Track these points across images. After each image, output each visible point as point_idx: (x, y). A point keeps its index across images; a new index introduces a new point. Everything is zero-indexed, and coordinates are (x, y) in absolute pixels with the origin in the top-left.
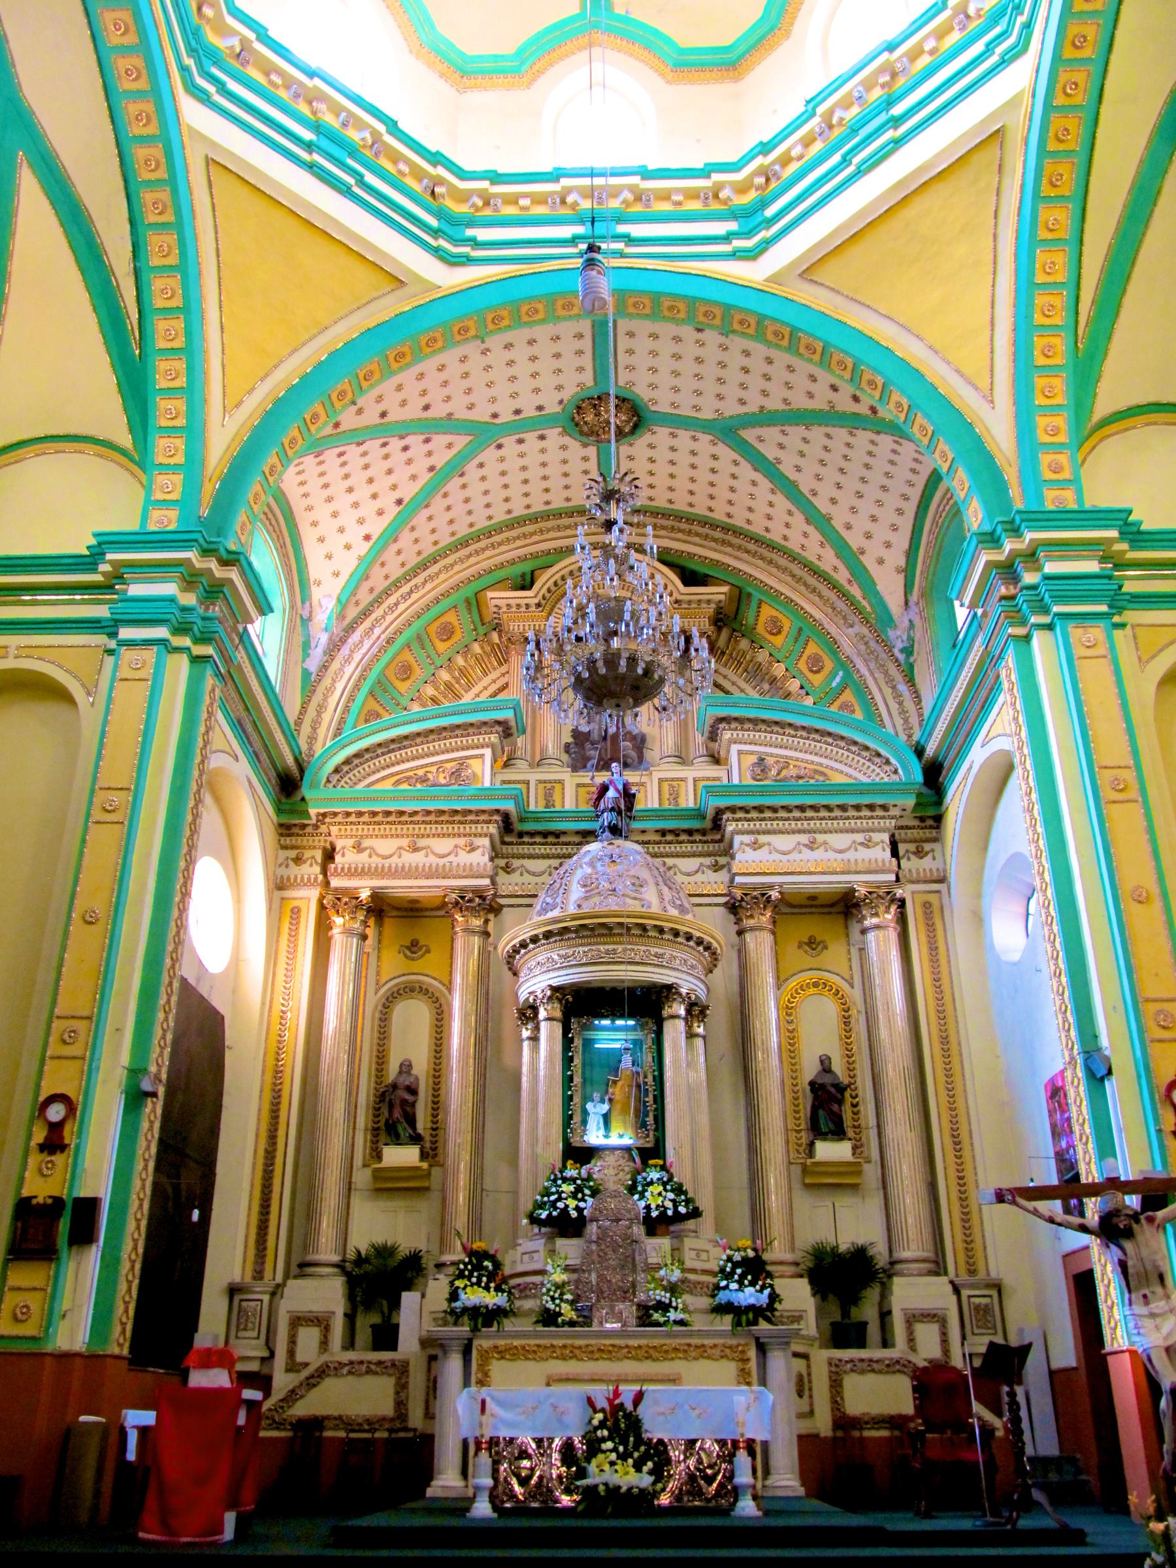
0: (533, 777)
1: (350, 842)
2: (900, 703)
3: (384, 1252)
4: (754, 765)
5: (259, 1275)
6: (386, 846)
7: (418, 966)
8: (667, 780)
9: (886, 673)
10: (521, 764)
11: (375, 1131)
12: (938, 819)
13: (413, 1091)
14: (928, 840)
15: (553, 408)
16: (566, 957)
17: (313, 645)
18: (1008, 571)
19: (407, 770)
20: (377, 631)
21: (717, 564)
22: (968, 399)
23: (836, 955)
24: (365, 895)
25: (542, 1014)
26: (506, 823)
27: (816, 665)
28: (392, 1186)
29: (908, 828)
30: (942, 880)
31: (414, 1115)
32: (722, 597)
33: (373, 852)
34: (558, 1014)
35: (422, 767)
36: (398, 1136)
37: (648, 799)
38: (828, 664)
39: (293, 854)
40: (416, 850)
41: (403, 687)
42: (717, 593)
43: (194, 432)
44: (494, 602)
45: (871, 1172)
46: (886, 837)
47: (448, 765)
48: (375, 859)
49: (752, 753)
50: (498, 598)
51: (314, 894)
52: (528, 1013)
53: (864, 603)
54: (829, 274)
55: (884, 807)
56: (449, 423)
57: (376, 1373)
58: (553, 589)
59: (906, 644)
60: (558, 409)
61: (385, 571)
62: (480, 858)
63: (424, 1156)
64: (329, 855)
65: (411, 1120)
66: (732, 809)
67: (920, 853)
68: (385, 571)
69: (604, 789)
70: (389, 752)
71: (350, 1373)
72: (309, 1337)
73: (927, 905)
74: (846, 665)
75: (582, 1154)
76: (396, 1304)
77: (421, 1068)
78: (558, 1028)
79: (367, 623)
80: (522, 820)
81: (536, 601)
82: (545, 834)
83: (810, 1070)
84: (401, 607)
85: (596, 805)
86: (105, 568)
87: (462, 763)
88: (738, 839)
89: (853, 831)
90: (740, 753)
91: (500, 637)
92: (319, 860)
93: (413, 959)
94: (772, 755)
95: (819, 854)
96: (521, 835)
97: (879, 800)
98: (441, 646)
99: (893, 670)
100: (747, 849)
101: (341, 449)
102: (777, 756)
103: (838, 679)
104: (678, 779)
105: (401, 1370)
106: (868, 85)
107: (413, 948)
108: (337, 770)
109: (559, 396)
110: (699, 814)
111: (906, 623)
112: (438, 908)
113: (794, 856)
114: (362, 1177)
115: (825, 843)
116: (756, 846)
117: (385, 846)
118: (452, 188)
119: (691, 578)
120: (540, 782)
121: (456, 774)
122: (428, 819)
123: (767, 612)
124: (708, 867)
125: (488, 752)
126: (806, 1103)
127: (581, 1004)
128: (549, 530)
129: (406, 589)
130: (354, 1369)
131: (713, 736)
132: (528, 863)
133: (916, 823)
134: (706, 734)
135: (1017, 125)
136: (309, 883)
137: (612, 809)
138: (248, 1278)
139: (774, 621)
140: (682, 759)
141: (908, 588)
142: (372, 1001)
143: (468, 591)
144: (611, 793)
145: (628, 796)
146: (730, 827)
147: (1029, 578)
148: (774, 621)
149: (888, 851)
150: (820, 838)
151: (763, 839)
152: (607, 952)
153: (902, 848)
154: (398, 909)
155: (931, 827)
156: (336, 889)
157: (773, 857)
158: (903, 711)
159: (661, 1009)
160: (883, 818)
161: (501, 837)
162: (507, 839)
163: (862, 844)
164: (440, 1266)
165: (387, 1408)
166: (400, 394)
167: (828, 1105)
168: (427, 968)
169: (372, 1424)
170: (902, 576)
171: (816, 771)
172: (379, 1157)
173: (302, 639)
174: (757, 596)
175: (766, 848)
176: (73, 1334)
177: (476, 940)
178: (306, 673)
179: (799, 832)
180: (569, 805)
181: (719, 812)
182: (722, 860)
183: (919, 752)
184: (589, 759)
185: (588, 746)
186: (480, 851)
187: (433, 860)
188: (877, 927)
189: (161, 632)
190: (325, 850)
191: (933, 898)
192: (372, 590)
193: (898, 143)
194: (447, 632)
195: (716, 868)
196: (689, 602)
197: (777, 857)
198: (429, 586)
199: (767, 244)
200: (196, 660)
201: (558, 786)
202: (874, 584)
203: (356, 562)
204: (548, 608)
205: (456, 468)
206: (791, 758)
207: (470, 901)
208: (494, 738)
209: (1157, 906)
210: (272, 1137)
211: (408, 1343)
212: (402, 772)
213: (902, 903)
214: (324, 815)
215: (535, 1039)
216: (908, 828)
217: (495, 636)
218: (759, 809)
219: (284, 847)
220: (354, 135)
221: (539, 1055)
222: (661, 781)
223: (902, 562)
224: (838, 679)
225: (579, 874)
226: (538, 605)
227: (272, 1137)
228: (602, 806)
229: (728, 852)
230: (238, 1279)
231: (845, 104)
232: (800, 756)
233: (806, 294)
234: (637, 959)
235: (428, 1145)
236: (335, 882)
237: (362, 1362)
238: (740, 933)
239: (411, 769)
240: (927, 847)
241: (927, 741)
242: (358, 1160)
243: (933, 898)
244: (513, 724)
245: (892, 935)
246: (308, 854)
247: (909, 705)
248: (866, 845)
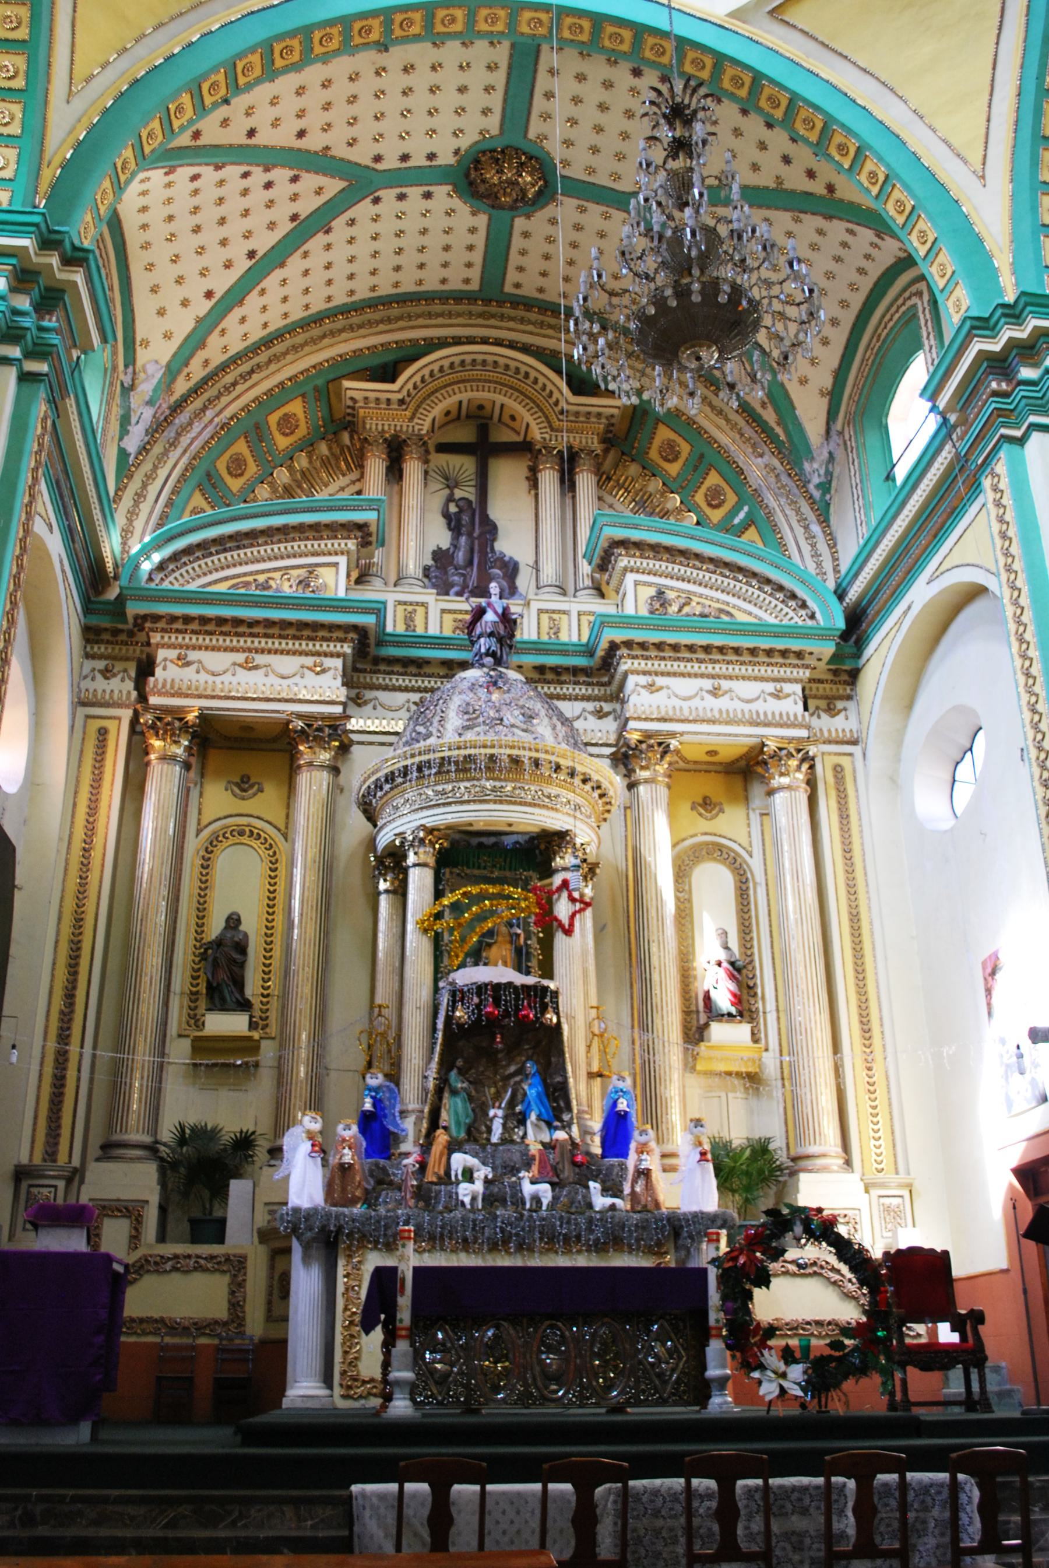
0: (391, 598)
2: (813, 546)
4: (652, 598)
5: (51, 1154)
8: (547, 611)
9: (798, 511)
10: (377, 583)
11: (194, 996)
12: (854, 675)
13: (242, 948)
14: (841, 698)
15: (447, 158)
16: (444, 793)
17: (133, 420)
19: (245, 574)
20: (210, 414)
24: (191, 717)
25: (411, 859)
29: (820, 681)
31: (243, 977)
32: (615, 411)
33: (201, 667)
35: (263, 572)
36: (223, 999)
37: (527, 631)
38: (731, 499)
44: (350, 393)
46: (798, 688)
47: (295, 573)
48: (203, 677)
49: (650, 584)
50: (355, 388)
52: (393, 861)
53: (779, 430)
55: (799, 655)
56: (322, 162)
57: (206, 1270)
58: (420, 385)
59: (823, 479)
60: (451, 160)
61: (224, 341)
63: (252, 1026)
66: (628, 644)
68: (224, 341)
69: (479, 613)
70: (225, 550)
71: (175, 1269)
73: (838, 770)
76: (221, 1193)
77: (252, 925)
79: (198, 403)
80: (380, 643)
81: (400, 396)
85: (470, 634)
87: (311, 568)
88: (632, 680)
89: (763, 679)
90: (637, 583)
91: (352, 438)
92: (133, 674)
93: (243, 799)
94: (672, 589)
95: (723, 703)
96: (377, 660)
97: (795, 645)
98: (283, 442)
99: (806, 509)
100: (643, 691)
101: (196, 170)
102: (679, 590)
103: (742, 515)
104: (559, 612)
105: (236, 1265)
109: (455, 143)
111: (826, 455)
112: (275, 739)
113: (696, 702)
114: (180, 1051)
115: (730, 691)
116: (651, 688)
120: (400, 603)
121: (304, 583)
122: (270, 631)
123: (663, 434)
124: (592, 713)
125: (342, 560)
128: (418, 316)
130: (178, 1265)
131: (604, 564)
132: (381, 695)
133: (830, 677)
134: (596, 560)
137: (491, 635)
138: (37, 1160)
139: (671, 445)
141: (832, 415)
142: (193, 844)
144: (490, 617)
145: (508, 620)
146: (625, 665)
148: (671, 445)
149: (801, 704)
150: (725, 684)
152: (494, 789)
153: (812, 703)
154: (227, 738)
155: (846, 683)
156: (156, 708)
158: (816, 555)
159: (551, 859)
160: (795, 666)
161: (354, 662)
162: (359, 666)
163: (771, 694)
166: (273, 110)
169: (201, 1327)
170: (825, 401)
171: (721, 611)
172: (200, 1025)
173: (121, 412)
175: (664, 692)
177: (325, 776)
179: (702, 676)
180: (433, 630)
181: (613, 647)
183: (840, 594)
184: (452, 585)
185: (451, 570)
186: (332, 672)
188: (789, 788)
190: (139, 662)
191: (845, 761)
192: (206, 362)
195: (600, 714)
196: (577, 414)
197: (678, 703)
200: (25, 378)
201: (420, 610)
202: (794, 408)
203: (191, 325)
204: (412, 406)
205: (319, 222)
206: (695, 594)
207: (320, 729)
208: (352, 545)
210: (70, 996)
211: (240, 1235)
212: (238, 576)
214: (145, 617)
216: (820, 681)
217: (346, 437)
218: (659, 646)
219: (88, 656)
222: (540, 611)
223: (828, 382)
224: (742, 515)
225: (456, 701)
226: (402, 402)
227: (70, 996)
228: (478, 630)
229: (618, 696)
230: (24, 1160)
232: (703, 593)
234: (529, 799)
235: (257, 1013)
236: (153, 700)
237: (189, 1257)
238: (631, 786)
239: (251, 573)
240: (840, 705)
241: (851, 583)
242: (173, 1029)
243: (845, 761)
244: (373, 529)
245: (802, 797)
247: (822, 547)
248: (777, 695)
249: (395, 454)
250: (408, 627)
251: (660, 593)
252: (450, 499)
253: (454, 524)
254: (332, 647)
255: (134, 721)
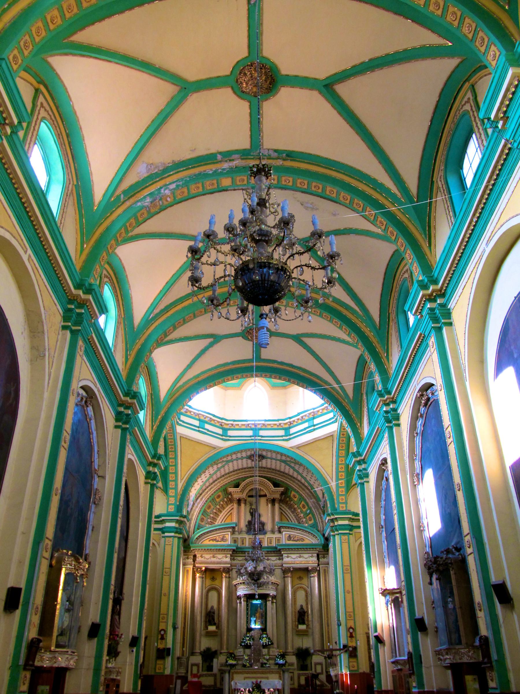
1: (199, 555)
3: (208, 649)
6: (207, 556)
7: (214, 583)
9: (319, 512)
10: (237, 533)
11: (206, 622)
13: (214, 613)
18: (332, 520)
21: (281, 481)
22: (328, 479)
23: (305, 581)
26: (234, 550)
27: (304, 506)
28: (209, 634)
30: (328, 564)
33: (205, 558)
34: (245, 600)
39: (186, 556)
40: (214, 557)
41: (209, 511)
42: (281, 489)
43: (176, 488)
45: (310, 631)
46: (316, 555)
50: (231, 490)
51: (191, 567)
52: (239, 598)
54: (302, 449)
55: (316, 549)
62: (228, 560)
63: (217, 628)
64: (195, 556)
65: (214, 620)
66: (283, 549)
67: (324, 557)
72: (195, 669)
73: (325, 570)
74: (310, 508)
75: (249, 630)
76: (212, 661)
77: (215, 607)
78: (245, 602)
82: (242, 552)
83: (298, 608)
84: (209, 493)
86: (161, 519)
95: (301, 559)
97: (314, 547)
98: (218, 500)
105: (215, 675)
106: (310, 414)
107: (213, 579)
108: (197, 538)
110: (276, 548)
113: (296, 559)
114: (203, 632)
116: (288, 557)
117: (207, 556)
118: (225, 424)
119: (276, 485)
123: (293, 493)
125: (229, 533)
126: (297, 616)
127: (250, 597)
129: (210, 488)
130: (206, 675)
135: (335, 435)
136: (191, 564)
138: (181, 656)
140: (273, 532)
143: (224, 488)
147: (336, 523)
151: (289, 555)
153: (320, 556)
157: (292, 560)
164: (221, 653)
165: (212, 683)
167: (302, 616)
168: (216, 583)
169: (210, 686)
174: (290, 489)
176: (168, 672)
177: (228, 579)
178: (188, 511)
180: (247, 545)
182: (281, 557)
183: (324, 535)
187: (218, 560)
189: (173, 534)
191: (326, 568)
193: (314, 430)
194: (219, 496)
195: (279, 559)
198: (215, 487)
199: (290, 439)
208: (231, 530)
209: (351, 594)
210: (185, 624)
211: (215, 670)
213: (319, 570)
215: (240, 603)
220: (207, 419)
221: (242, 606)
227: (185, 624)
231: (305, 416)
233: (298, 451)
238: (284, 577)
240: (326, 556)
243: (326, 568)
246: (190, 557)
249: (239, 501)
250: (243, 544)
251: (290, 536)
252: (251, 508)
253: (252, 514)
254: (228, 552)
255: (193, 569)
